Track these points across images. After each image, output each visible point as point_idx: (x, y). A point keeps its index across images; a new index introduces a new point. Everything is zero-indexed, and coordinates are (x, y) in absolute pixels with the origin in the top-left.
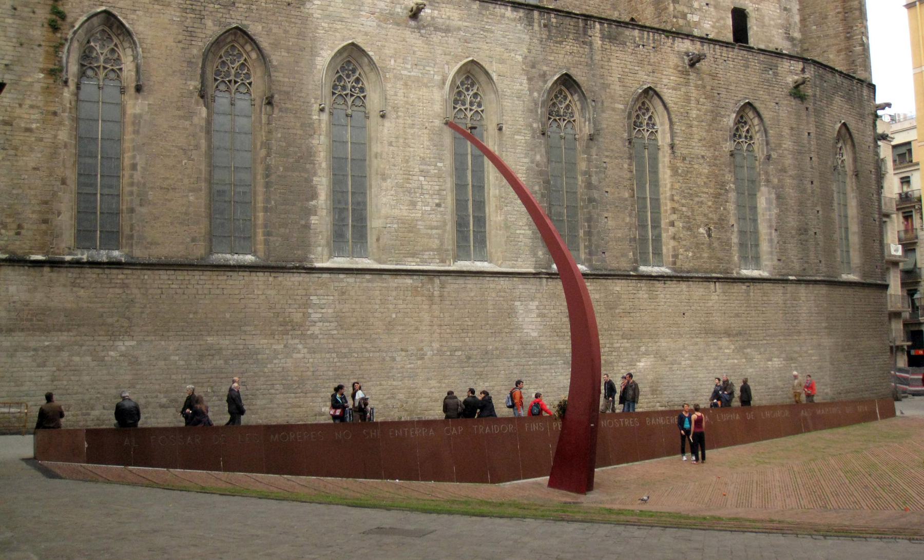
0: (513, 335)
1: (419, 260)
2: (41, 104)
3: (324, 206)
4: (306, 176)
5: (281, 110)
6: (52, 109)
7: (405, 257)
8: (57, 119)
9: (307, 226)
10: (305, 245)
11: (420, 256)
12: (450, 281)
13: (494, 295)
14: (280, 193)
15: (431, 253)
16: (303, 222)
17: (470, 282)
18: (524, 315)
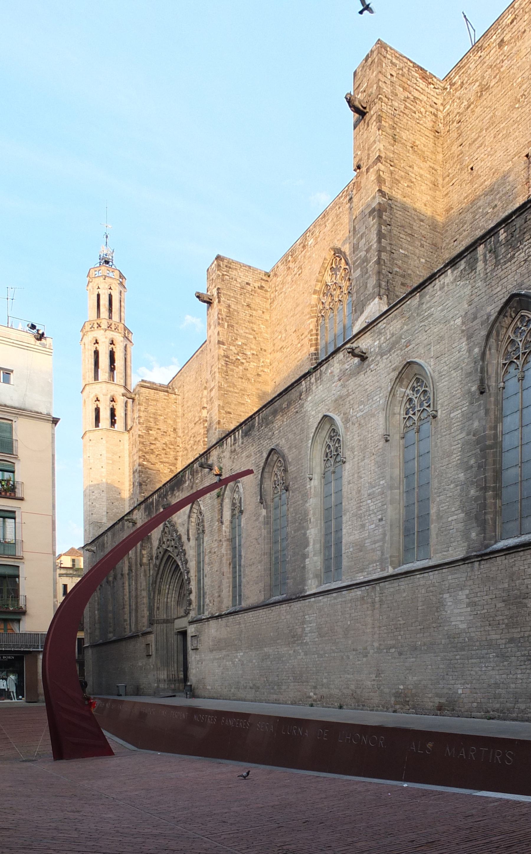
0: (440, 629)
1: (366, 573)
2: (217, 538)
3: (312, 550)
4: (303, 532)
5: (293, 492)
6: (219, 539)
7: (357, 573)
8: (221, 543)
9: (304, 567)
10: (303, 581)
11: (367, 570)
12: (387, 587)
13: (423, 591)
14: (292, 549)
15: (375, 565)
16: (302, 565)
17: (403, 583)
18: (453, 607)
